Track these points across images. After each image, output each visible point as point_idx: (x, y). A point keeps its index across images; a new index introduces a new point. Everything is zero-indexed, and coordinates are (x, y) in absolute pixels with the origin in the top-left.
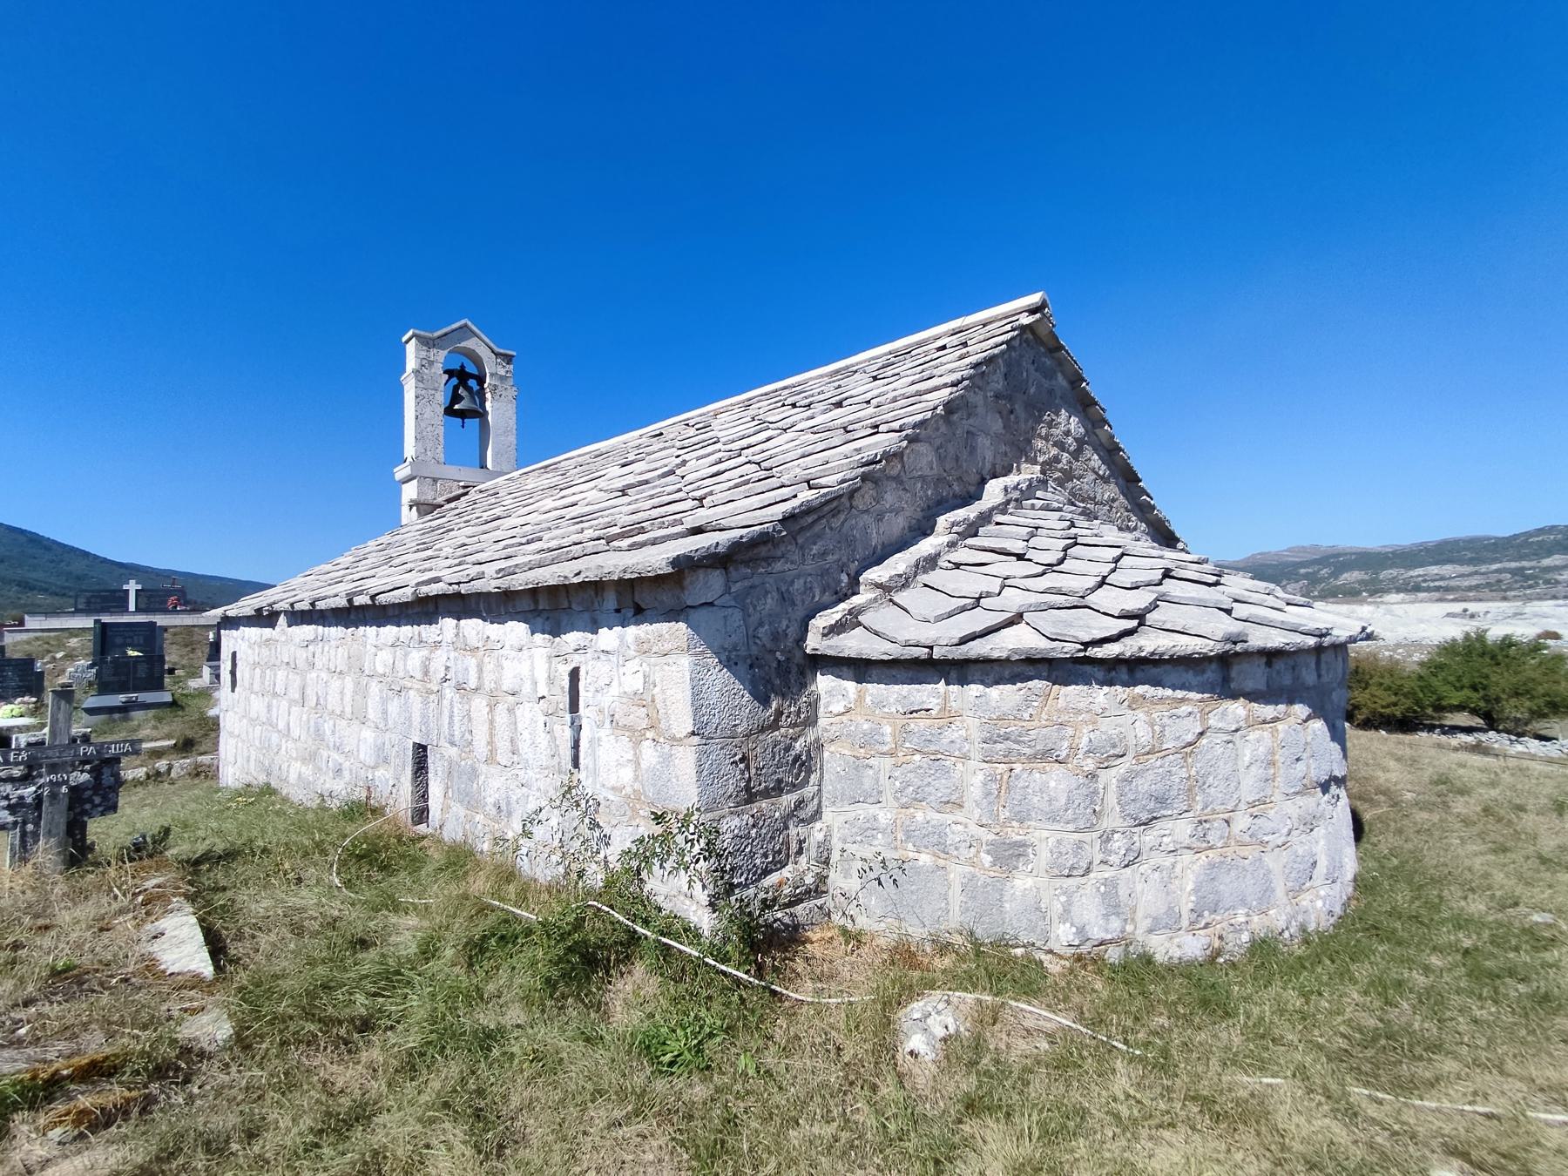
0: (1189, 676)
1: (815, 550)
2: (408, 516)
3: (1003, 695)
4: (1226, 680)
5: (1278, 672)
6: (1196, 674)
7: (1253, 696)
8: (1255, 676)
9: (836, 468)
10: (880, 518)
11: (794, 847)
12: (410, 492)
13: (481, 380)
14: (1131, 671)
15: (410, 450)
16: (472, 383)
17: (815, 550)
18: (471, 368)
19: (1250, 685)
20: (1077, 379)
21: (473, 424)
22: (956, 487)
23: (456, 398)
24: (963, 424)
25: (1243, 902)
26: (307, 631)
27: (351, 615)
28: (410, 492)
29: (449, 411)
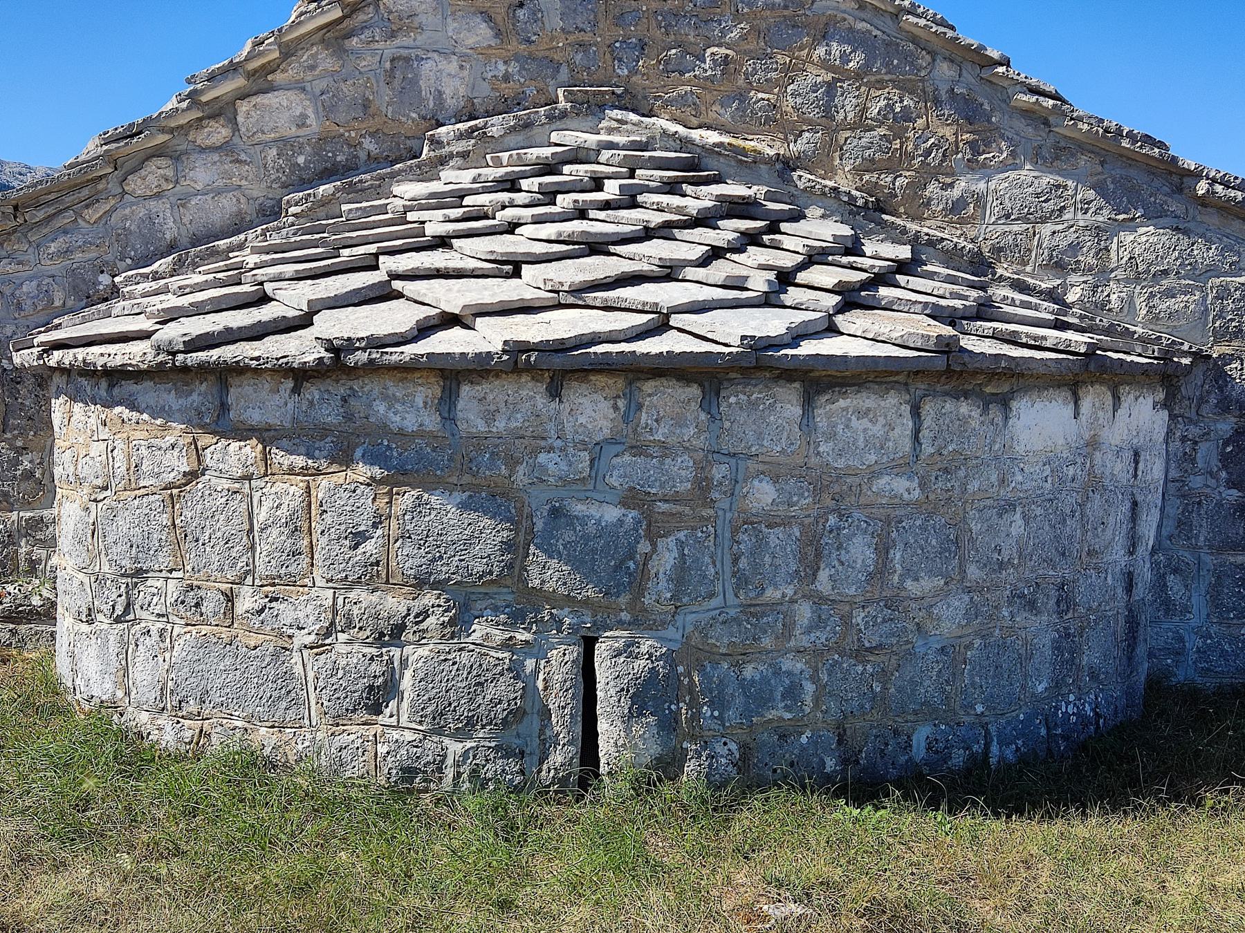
0: (171, 399)
1: (53, 247)
4: (224, 407)
5: (311, 403)
6: (179, 394)
7: (267, 436)
10: (183, 201)
11: (23, 566)
14: (111, 386)
17: (53, 247)
19: (255, 417)
22: (369, 145)
25: (241, 701)
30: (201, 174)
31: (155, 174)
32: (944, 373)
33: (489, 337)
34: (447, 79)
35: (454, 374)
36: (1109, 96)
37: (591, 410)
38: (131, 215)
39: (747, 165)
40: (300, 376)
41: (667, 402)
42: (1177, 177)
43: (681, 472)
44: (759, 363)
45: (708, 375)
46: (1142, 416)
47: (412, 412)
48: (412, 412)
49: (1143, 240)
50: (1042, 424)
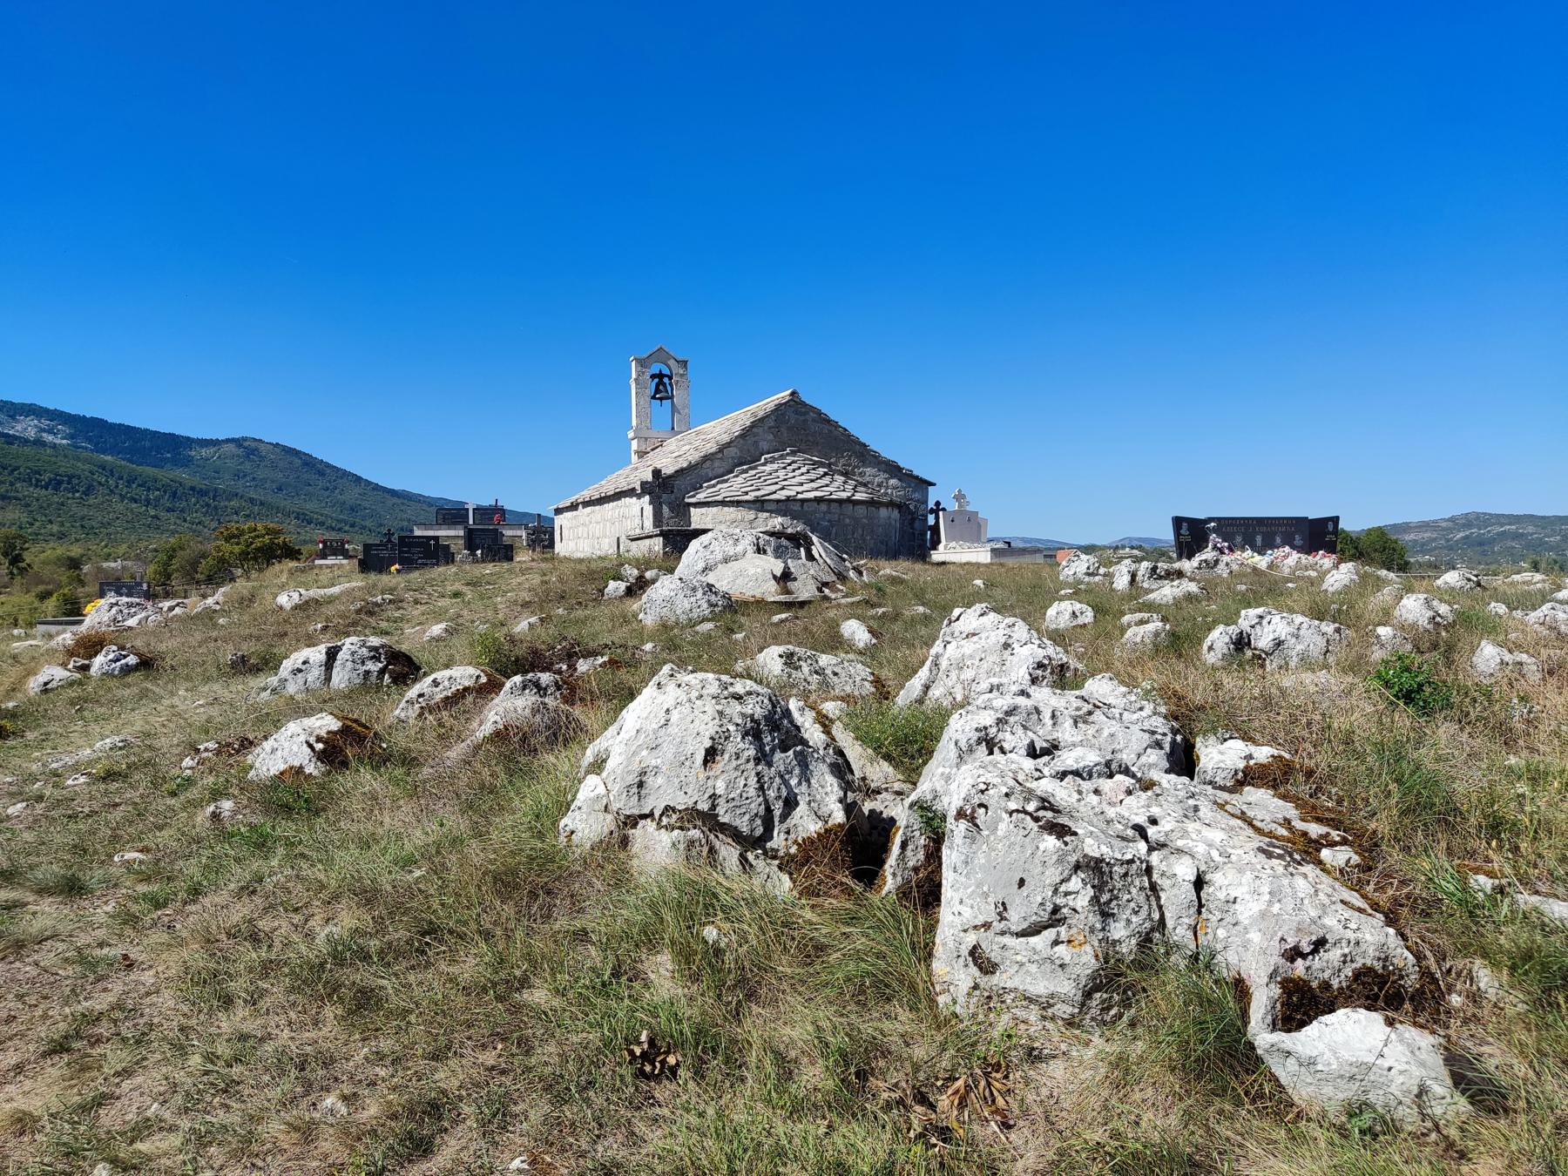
2: (634, 458)
3: (715, 509)
7: (771, 512)
8: (773, 506)
9: (694, 457)
12: (634, 445)
13: (670, 378)
15: (634, 423)
16: (666, 380)
18: (666, 371)
20: (819, 413)
21: (667, 403)
23: (657, 391)
24: (750, 440)
26: (589, 509)
27: (602, 500)
28: (634, 445)
29: (653, 397)
30: (717, 464)
31: (708, 463)
32: (871, 503)
33: (811, 495)
34: (764, 445)
36: (887, 453)
37: (823, 507)
38: (703, 472)
39: (822, 465)
40: (778, 501)
42: (900, 469)
44: (849, 500)
45: (840, 501)
46: (896, 512)
47: (797, 507)
48: (797, 507)
49: (893, 482)
50: (883, 512)
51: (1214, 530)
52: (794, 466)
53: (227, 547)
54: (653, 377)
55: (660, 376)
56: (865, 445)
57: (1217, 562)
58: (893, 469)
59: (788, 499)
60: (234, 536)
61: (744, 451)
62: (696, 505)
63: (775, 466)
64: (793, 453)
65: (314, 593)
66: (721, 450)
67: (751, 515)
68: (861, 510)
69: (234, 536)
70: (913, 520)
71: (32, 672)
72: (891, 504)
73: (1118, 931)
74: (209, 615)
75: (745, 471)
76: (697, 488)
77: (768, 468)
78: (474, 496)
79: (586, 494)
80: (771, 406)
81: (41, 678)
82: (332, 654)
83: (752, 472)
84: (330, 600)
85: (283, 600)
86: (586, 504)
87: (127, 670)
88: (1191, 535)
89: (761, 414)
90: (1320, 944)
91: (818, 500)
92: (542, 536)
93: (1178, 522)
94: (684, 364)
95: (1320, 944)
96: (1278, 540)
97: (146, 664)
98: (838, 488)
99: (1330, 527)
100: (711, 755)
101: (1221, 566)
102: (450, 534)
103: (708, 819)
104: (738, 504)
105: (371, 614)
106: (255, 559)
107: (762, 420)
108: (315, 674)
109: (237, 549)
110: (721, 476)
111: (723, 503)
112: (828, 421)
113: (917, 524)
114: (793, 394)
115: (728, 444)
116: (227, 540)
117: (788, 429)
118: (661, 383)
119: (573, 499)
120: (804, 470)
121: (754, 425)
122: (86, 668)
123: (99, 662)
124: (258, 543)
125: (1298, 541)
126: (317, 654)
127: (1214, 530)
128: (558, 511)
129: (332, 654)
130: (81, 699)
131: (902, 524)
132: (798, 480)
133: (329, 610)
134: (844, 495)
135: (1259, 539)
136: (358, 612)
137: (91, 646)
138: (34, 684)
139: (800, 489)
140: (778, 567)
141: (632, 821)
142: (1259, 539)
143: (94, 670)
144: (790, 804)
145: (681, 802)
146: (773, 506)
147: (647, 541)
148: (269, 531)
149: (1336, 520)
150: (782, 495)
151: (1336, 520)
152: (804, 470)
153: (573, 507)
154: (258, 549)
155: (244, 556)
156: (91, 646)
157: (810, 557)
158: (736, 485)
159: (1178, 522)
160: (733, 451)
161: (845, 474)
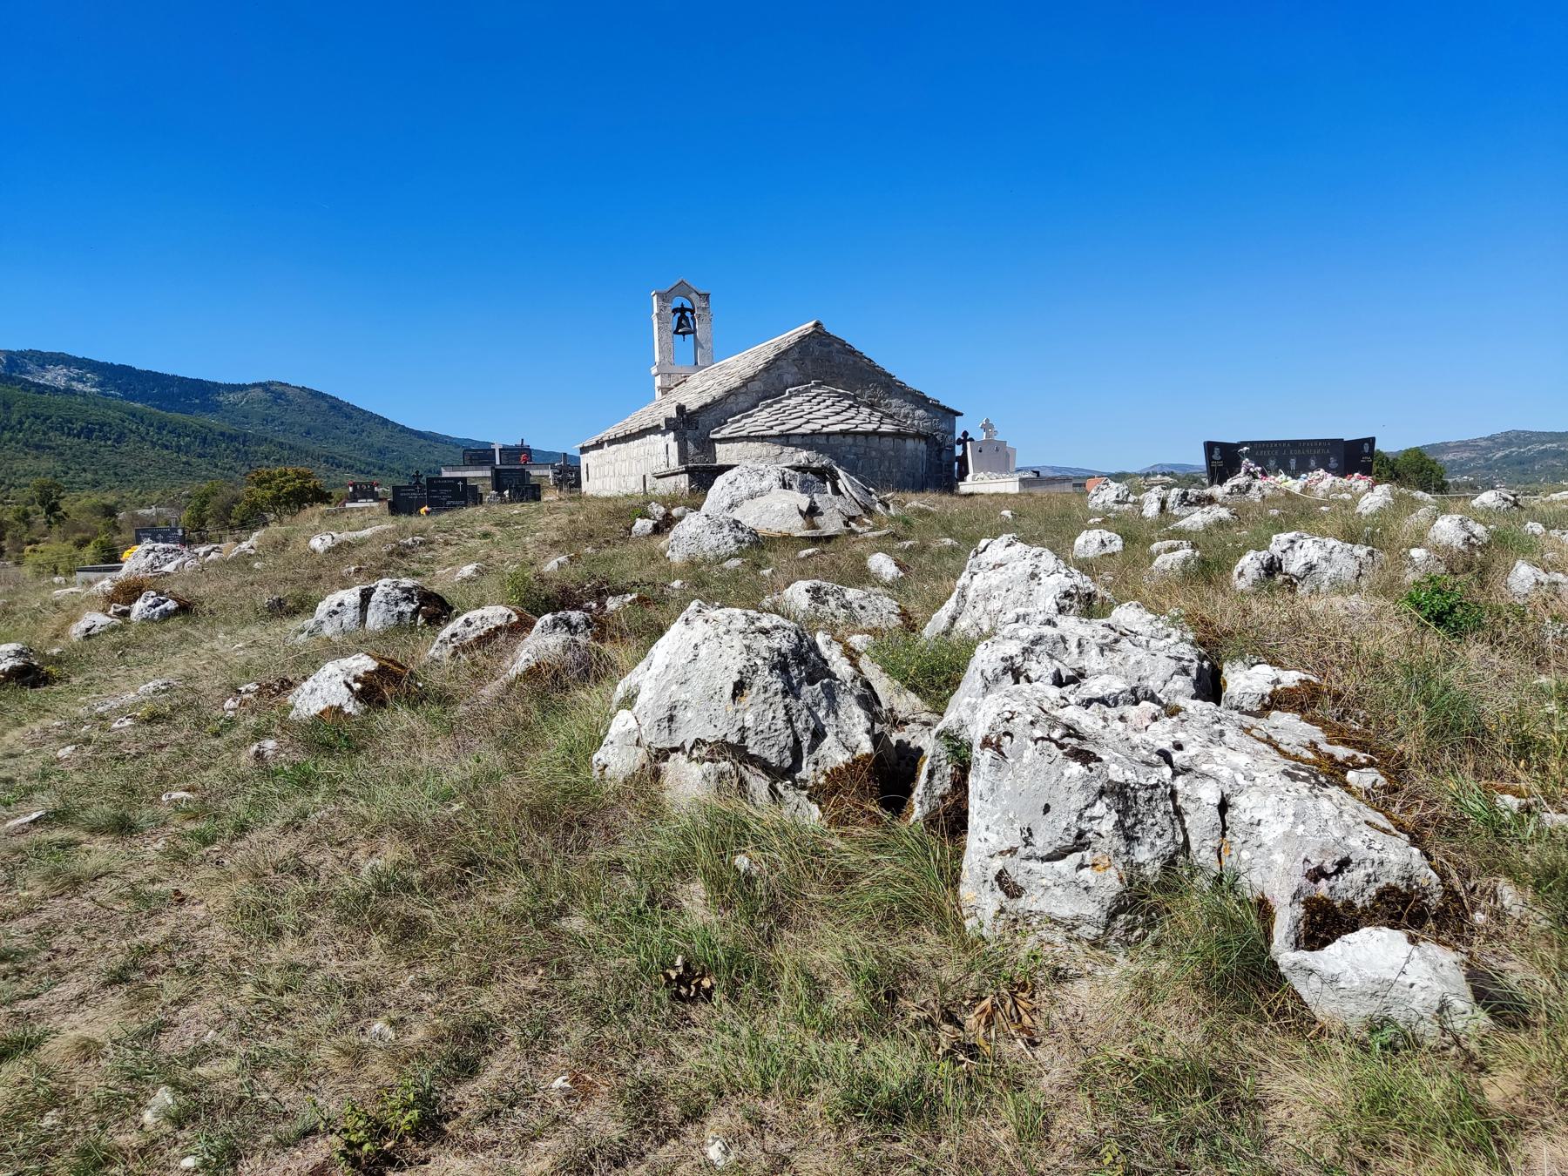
2: (658, 394)
8: (798, 441)
9: (718, 392)
13: (693, 312)
15: (657, 359)
16: (688, 314)
18: (688, 305)
20: (843, 343)
21: (690, 337)
23: (679, 325)
24: (774, 373)
26: (614, 447)
27: (627, 438)
29: (676, 332)
30: (741, 398)
32: (897, 435)
33: (837, 428)
34: (788, 378)
35: (829, 434)
36: (913, 384)
37: (849, 440)
39: (847, 397)
40: (804, 435)
41: (860, 438)
42: (926, 399)
43: (862, 450)
44: (875, 432)
45: (866, 434)
46: (922, 445)
48: (822, 441)
49: (920, 412)
50: (910, 444)
51: (1247, 454)
52: (819, 399)
53: (258, 492)
54: (675, 311)
55: (682, 310)
56: (890, 376)
57: (1249, 487)
58: (920, 400)
59: (814, 432)
60: (265, 481)
61: (767, 385)
62: (721, 441)
63: (800, 399)
64: (818, 386)
65: (346, 536)
66: (744, 385)
67: (776, 449)
68: (888, 442)
69: (265, 481)
70: (940, 451)
71: (73, 619)
72: (918, 435)
73: (1142, 854)
74: (244, 560)
75: (770, 405)
76: (721, 423)
77: (793, 401)
78: (500, 437)
79: (611, 432)
80: (795, 338)
81: (83, 625)
82: (366, 596)
83: (777, 406)
84: (363, 543)
85: (316, 543)
86: (612, 442)
87: (166, 615)
88: (1224, 459)
89: (784, 346)
90: (1344, 864)
91: (844, 433)
92: (569, 475)
93: (1210, 447)
94: (707, 296)
95: (1344, 864)
96: (1313, 463)
97: (185, 608)
98: (863, 420)
99: (1366, 448)
100: (739, 688)
101: (1254, 490)
102: (478, 475)
103: (738, 752)
104: (763, 438)
105: (403, 555)
106: (287, 503)
107: (785, 352)
108: (350, 616)
109: (268, 494)
110: (746, 411)
111: (748, 438)
112: (853, 352)
113: (944, 455)
114: (817, 325)
115: (753, 378)
116: (258, 485)
117: (813, 361)
118: (683, 317)
119: (598, 437)
120: (829, 402)
121: (777, 358)
122: (126, 614)
123: (139, 607)
124: (289, 487)
125: (1333, 463)
126: (351, 596)
127: (1247, 454)
128: (584, 450)
129: (366, 596)
130: (122, 644)
131: (929, 455)
132: (823, 412)
133: (361, 553)
134: (870, 427)
135: (1293, 462)
136: (390, 554)
137: (130, 592)
138: (76, 631)
139: (825, 422)
140: (804, 502)
141: (664, 754)
142: (1293, 462)
143: (134, 616)
144: (818, 735)
145: (711, 734)
146: (798, 441)
147: (673, 479)
148: (299, 475)
149: (1371, 441)
150: (807, 429)
151: (1371, 441)
152: (829, 402)
153: (599, 445)
154: (289, 493)
155: (276, 500)
156: (130, 592)
157: (837, 491)
158: (761, 419)
159: (1210, 447)
160: (757, 386)
161: (871, 406)
